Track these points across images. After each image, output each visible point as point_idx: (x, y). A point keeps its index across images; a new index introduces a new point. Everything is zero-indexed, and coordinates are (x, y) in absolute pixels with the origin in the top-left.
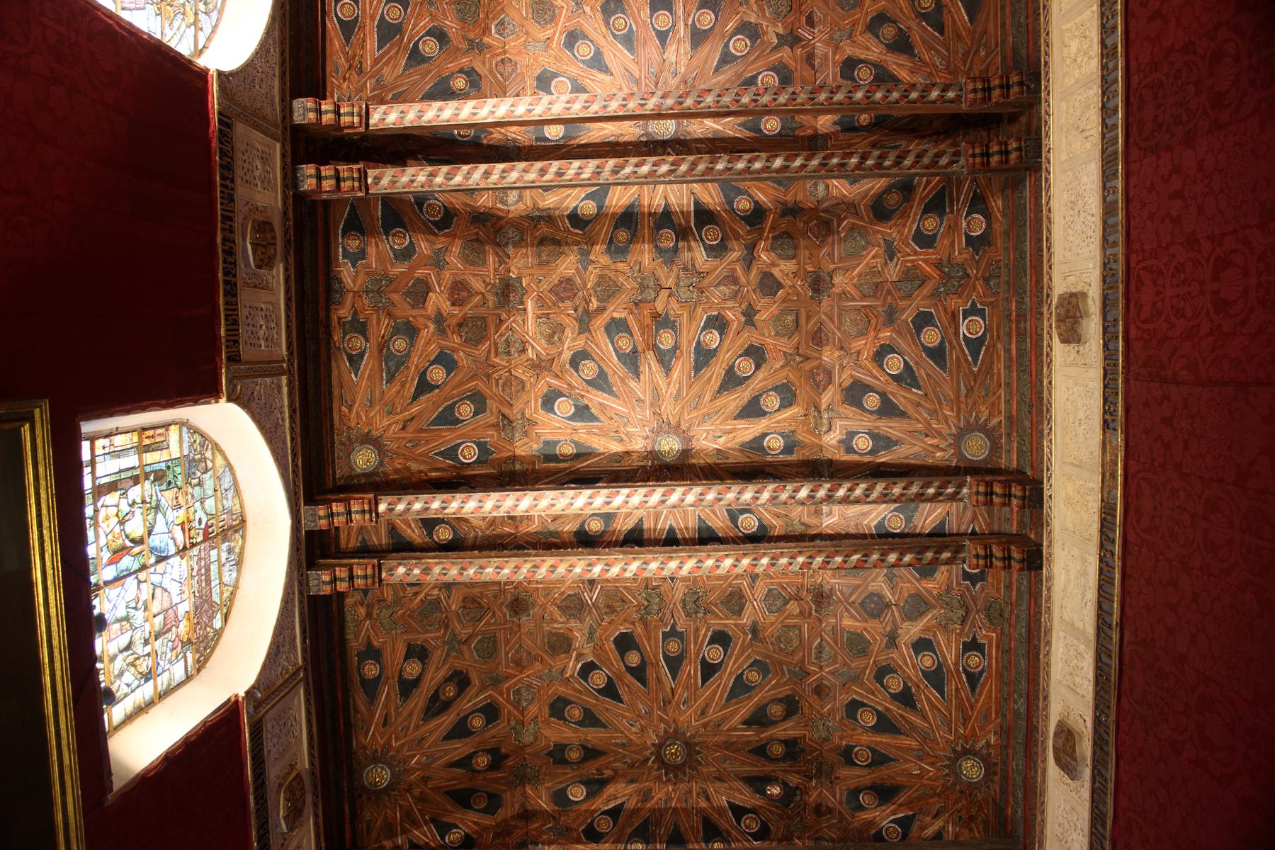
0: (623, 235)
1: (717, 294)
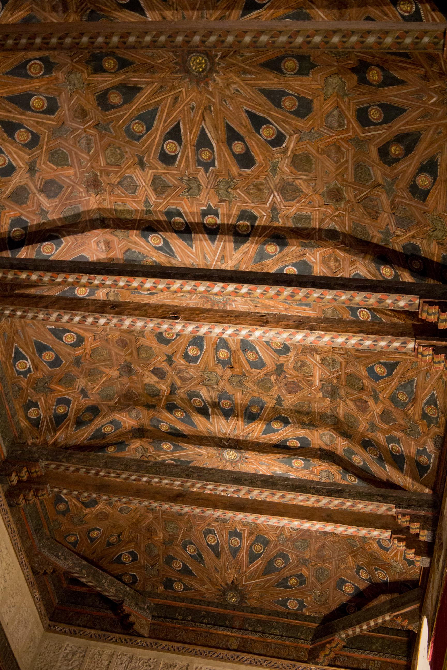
0: (254, 410)
1: (192, 372)
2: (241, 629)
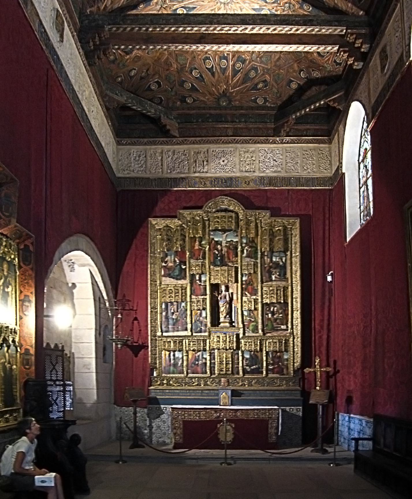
2: (232, 122)
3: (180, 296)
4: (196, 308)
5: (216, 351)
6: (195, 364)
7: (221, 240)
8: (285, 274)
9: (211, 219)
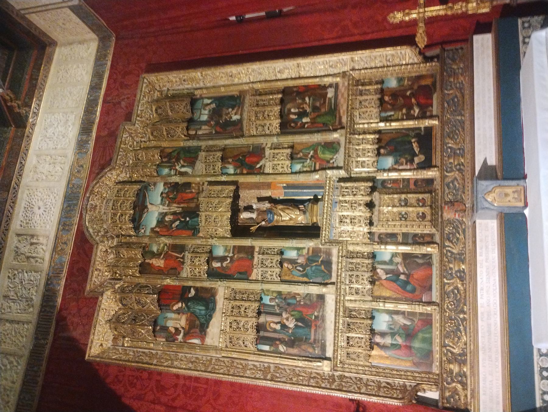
3: (247, 304)
4: (278, 270)
5: (374, 229)
6: (407, 283)
7: (156, 215)
8: (232, 98)
9: (117, 231)
